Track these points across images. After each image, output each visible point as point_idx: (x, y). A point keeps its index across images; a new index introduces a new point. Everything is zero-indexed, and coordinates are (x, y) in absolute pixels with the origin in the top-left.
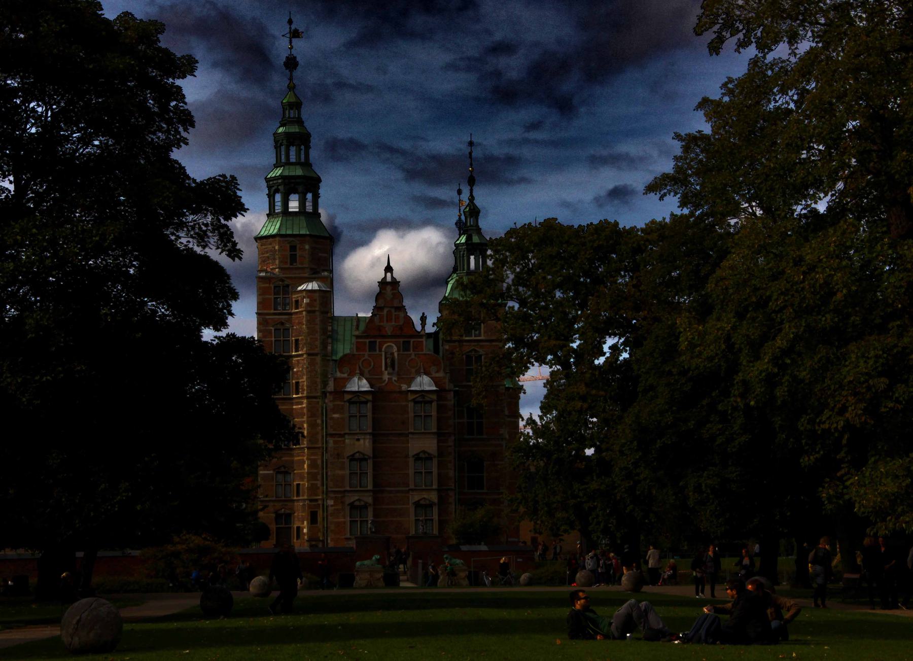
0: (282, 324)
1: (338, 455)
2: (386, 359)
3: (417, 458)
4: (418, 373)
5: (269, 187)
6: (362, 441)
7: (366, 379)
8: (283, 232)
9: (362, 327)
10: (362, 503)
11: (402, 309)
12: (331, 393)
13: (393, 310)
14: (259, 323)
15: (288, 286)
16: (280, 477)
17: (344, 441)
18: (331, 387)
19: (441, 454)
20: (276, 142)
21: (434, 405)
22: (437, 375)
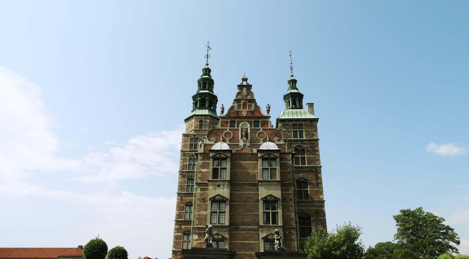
0: (193, 156)
1: (204, 199)
2: (242, 131)
3: (265, 200)
4: (265, 141)
5: (194, 100)
6: (222, 187)
7: (228, 145)
8: (197, 114)
9: (226, 112)
10: (220, 237)
11: (253, 101)
12: (201, 154)
13: (247, 102)
14: (182, 156)
15: (197, 138)
16: (186, 238)
17: (208, 188)
18: (201, 150)
19: (284, 199)
20: (199, 83)
21: (278, 160)
22: (279, 143)
